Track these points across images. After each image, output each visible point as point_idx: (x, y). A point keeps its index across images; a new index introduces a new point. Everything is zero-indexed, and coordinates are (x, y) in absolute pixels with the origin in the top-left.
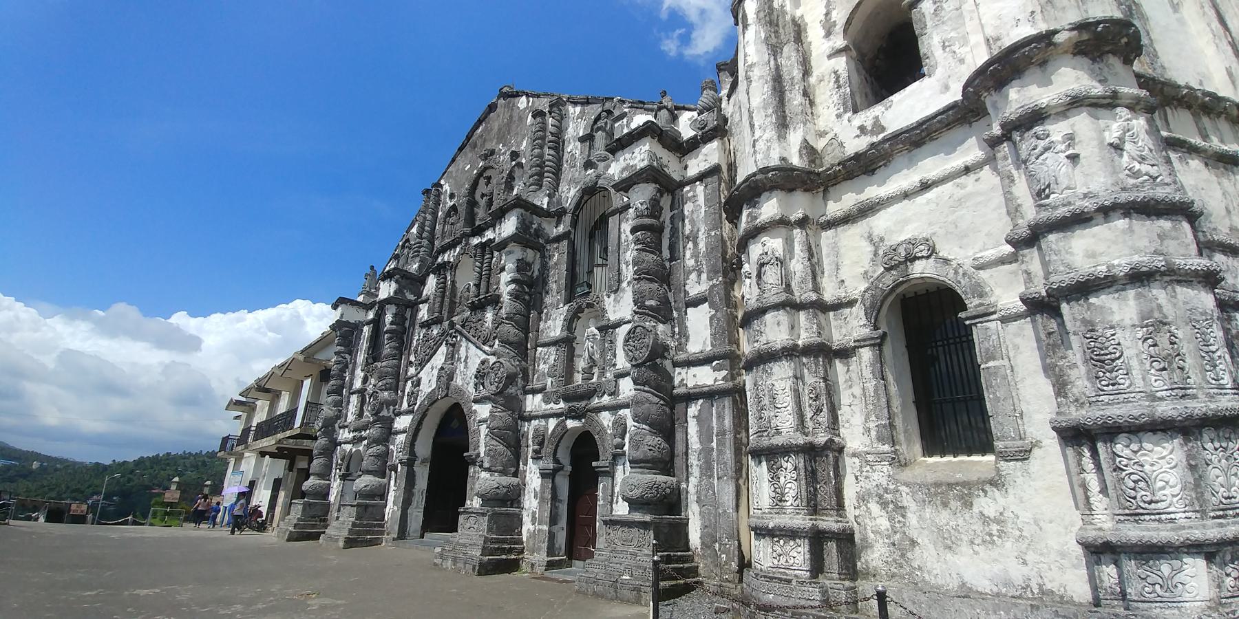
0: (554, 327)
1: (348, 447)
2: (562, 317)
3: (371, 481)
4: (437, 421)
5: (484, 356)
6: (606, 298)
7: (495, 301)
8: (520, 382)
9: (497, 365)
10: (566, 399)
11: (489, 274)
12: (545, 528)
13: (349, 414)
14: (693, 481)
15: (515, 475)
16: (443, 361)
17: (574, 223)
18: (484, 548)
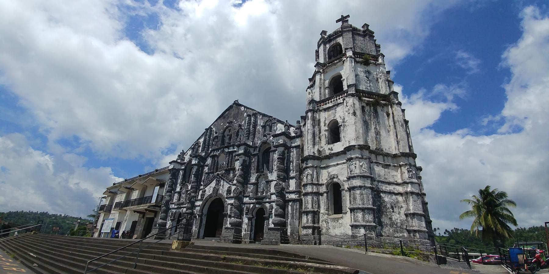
0: (253, 179)
1: (174, 211)
2: (255, 177)
4: (210, 202)
5: (229, 186)
6: (268, 174)
7: (234, 169)
8: (243, 194)
9: (237, 188)
10: (256, 199)
12: (249, 232)
14: (289, 220)
15: (240, 219)
16: (214, 185)
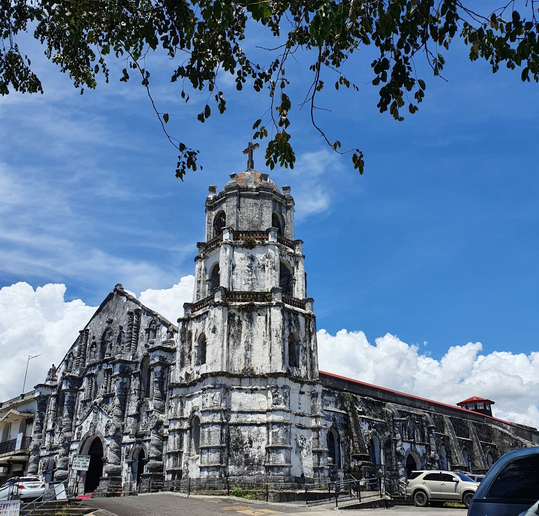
3: (62, 472)
8: (121, 431)
11: (111, 383)
13: (46, 442)
15: (119, 464)
16: (92, 419)
17: (141, 368)
18: (108, 489)
